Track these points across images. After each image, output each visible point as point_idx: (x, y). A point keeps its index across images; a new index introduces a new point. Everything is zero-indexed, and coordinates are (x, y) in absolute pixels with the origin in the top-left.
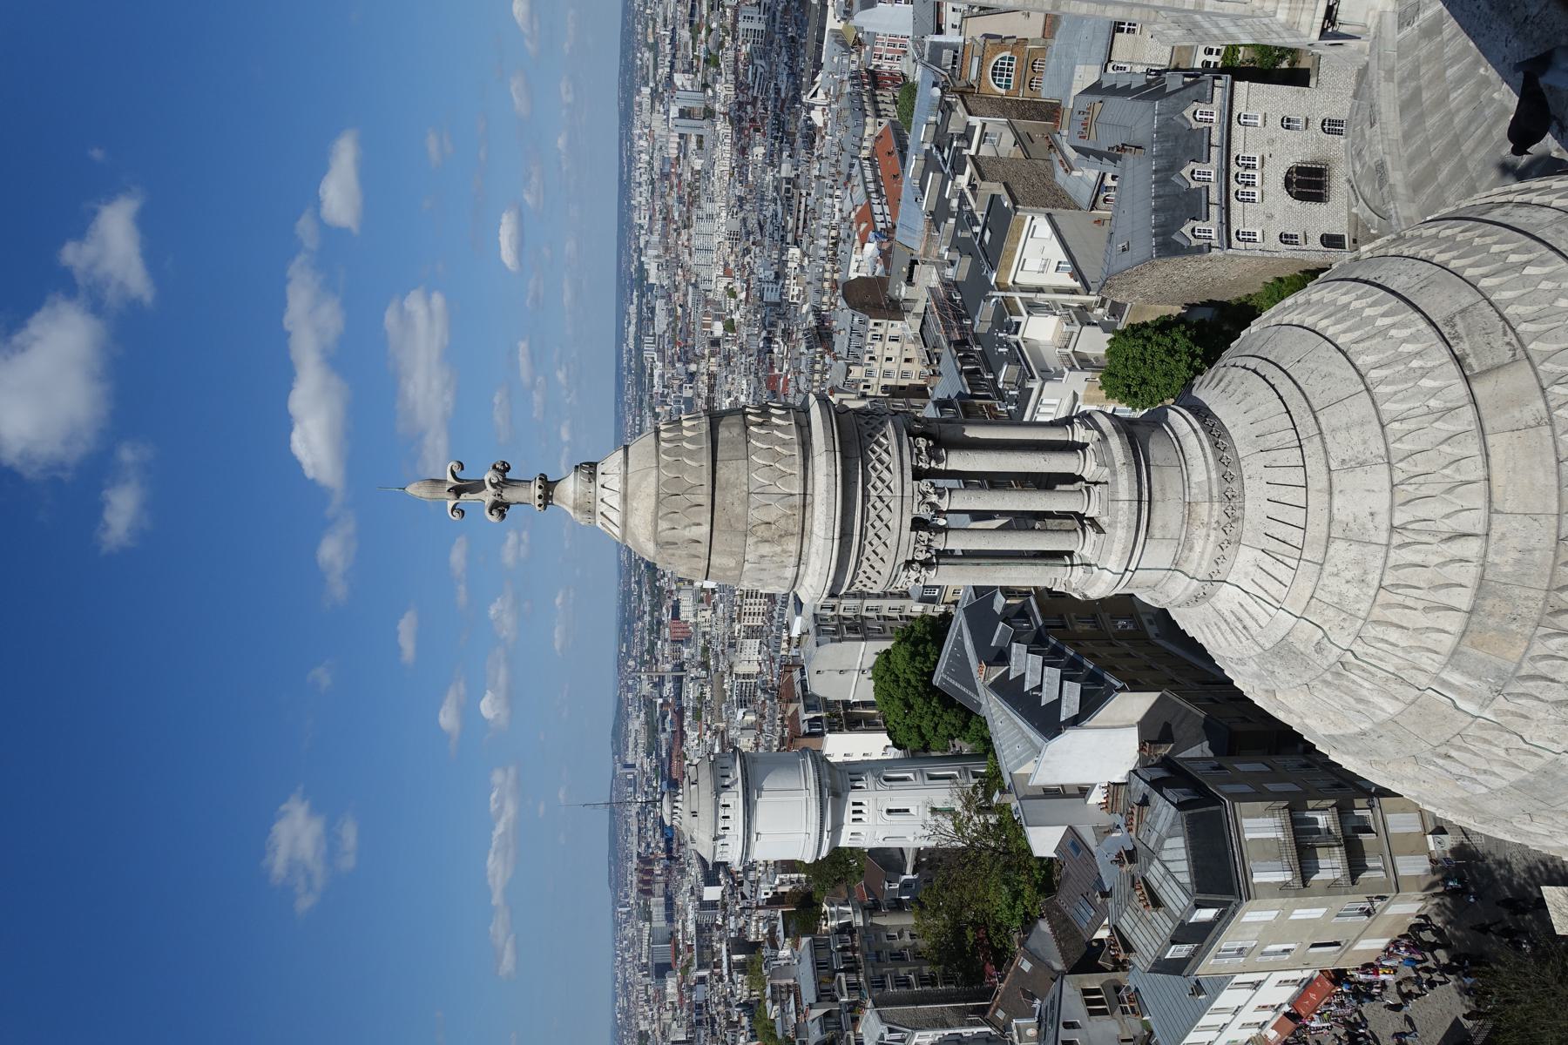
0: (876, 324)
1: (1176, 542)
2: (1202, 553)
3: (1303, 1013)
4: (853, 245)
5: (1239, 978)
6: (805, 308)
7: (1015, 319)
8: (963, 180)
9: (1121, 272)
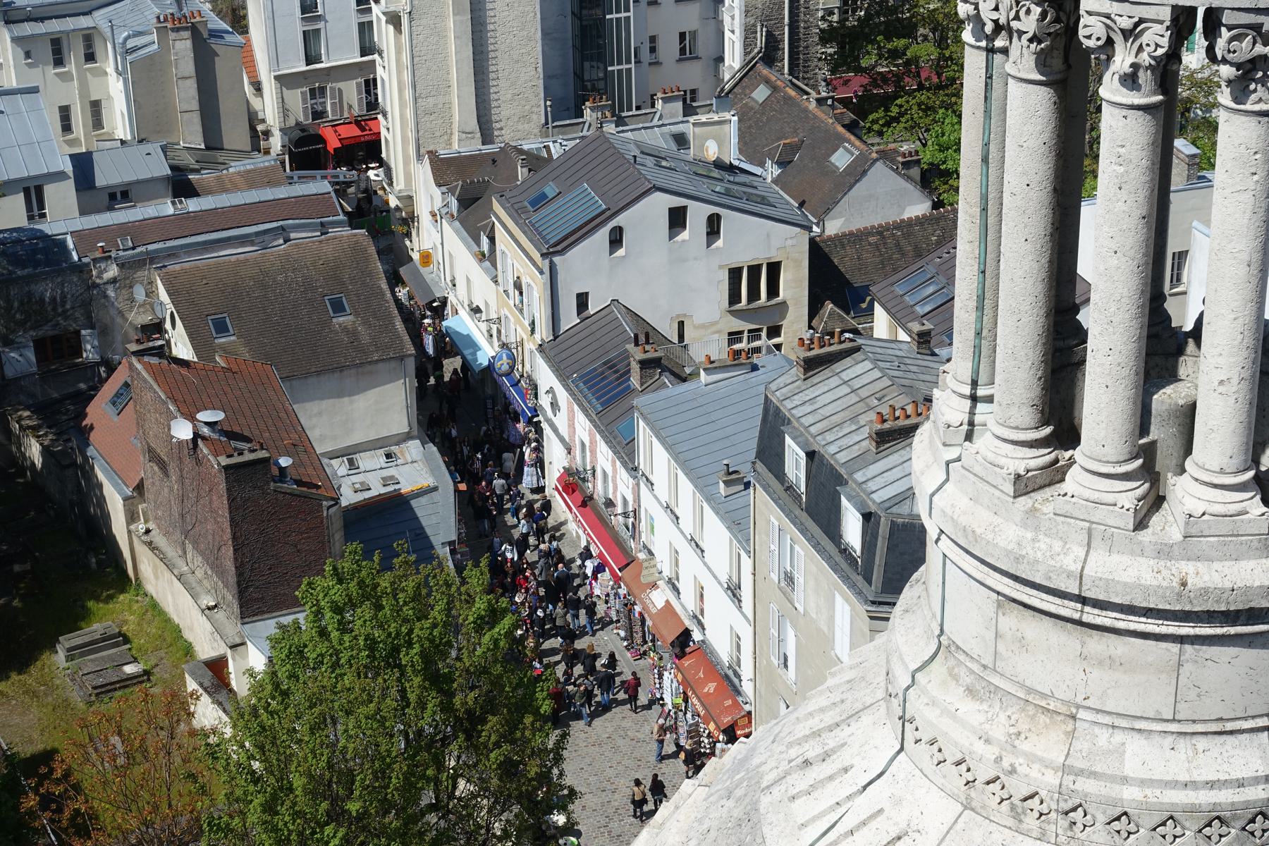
1: (988, 660)
2: (953, 715)
3: (686, 662)
5: (747, 563)
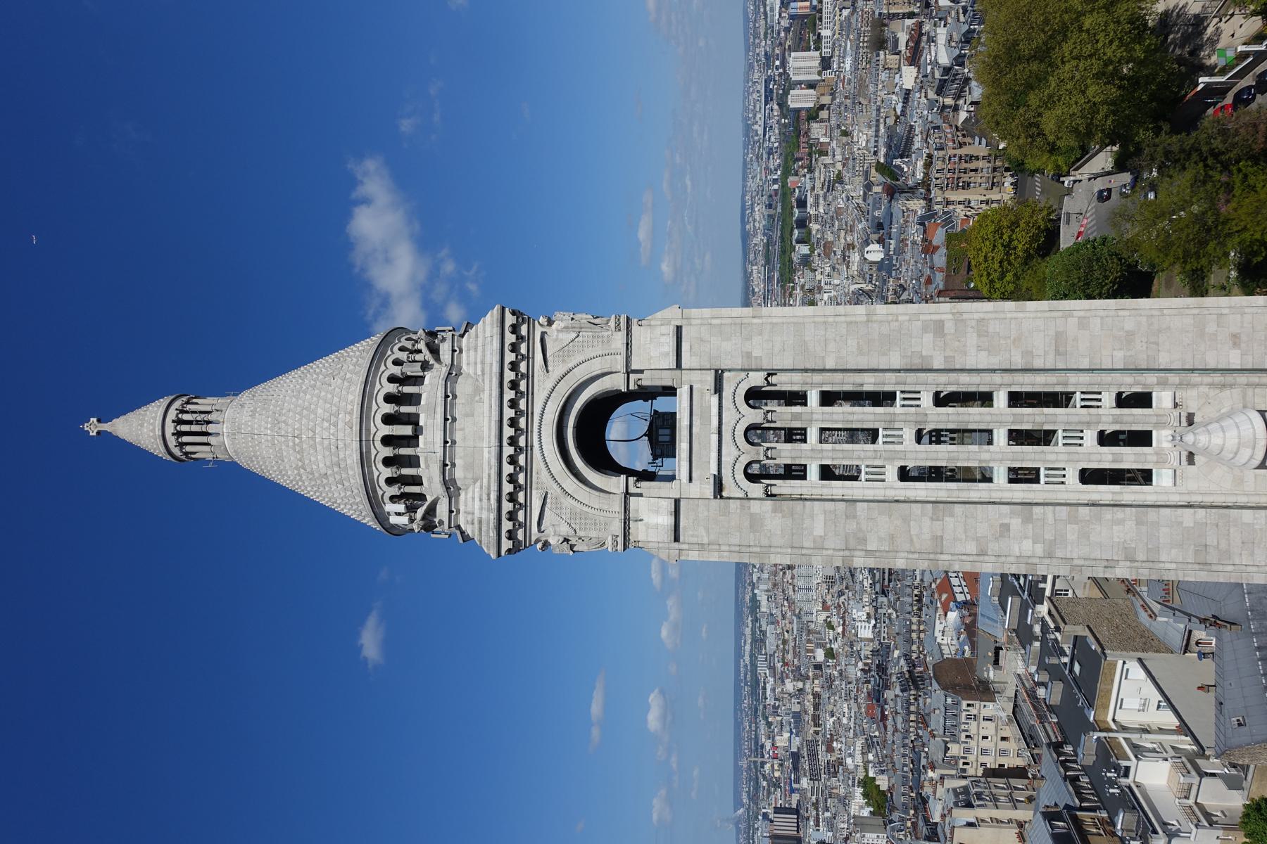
0: (969, 705)
4: (936, 612)
6: (896, 653)
7: (1124, 763)
8: (1043, 609)
9: (1240, 746)
